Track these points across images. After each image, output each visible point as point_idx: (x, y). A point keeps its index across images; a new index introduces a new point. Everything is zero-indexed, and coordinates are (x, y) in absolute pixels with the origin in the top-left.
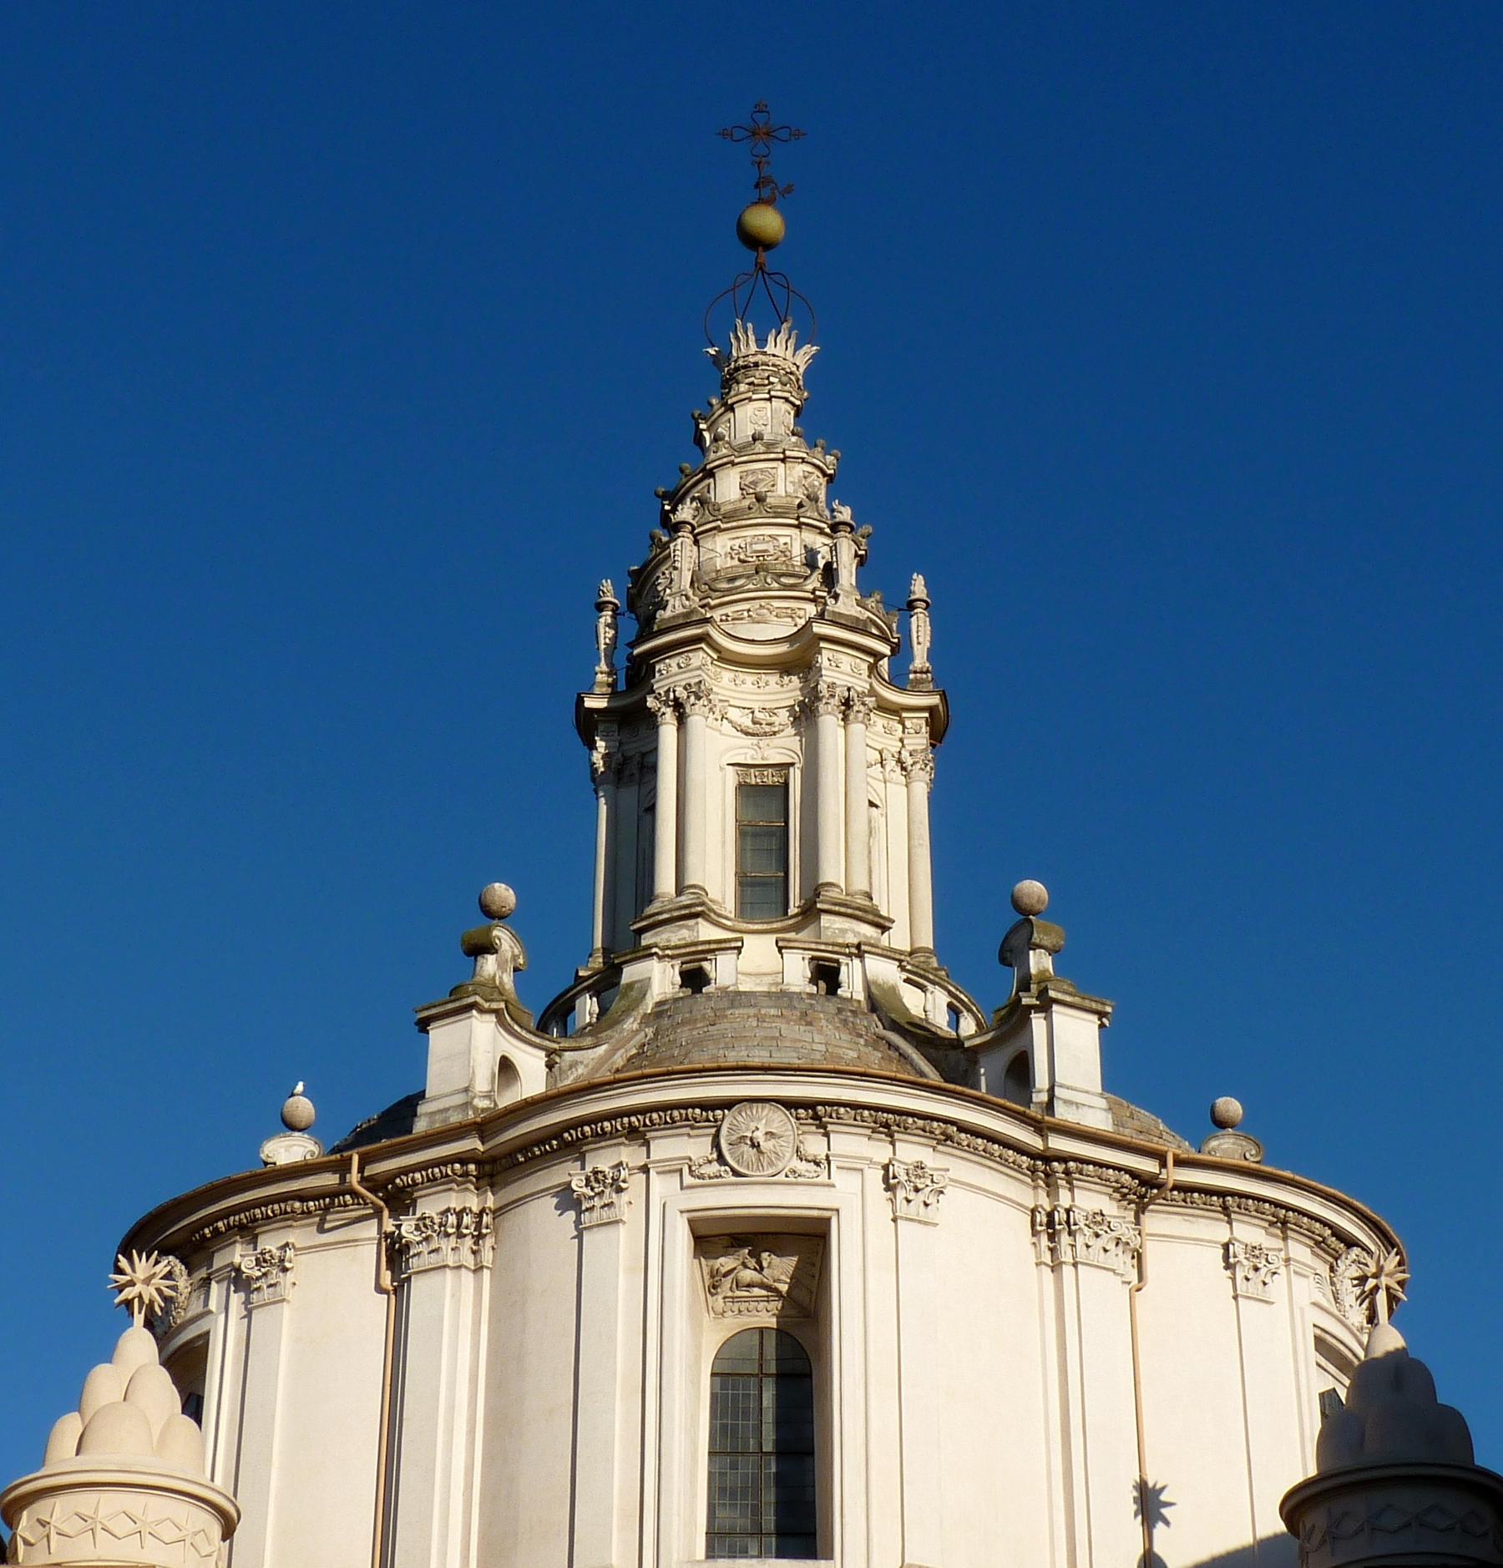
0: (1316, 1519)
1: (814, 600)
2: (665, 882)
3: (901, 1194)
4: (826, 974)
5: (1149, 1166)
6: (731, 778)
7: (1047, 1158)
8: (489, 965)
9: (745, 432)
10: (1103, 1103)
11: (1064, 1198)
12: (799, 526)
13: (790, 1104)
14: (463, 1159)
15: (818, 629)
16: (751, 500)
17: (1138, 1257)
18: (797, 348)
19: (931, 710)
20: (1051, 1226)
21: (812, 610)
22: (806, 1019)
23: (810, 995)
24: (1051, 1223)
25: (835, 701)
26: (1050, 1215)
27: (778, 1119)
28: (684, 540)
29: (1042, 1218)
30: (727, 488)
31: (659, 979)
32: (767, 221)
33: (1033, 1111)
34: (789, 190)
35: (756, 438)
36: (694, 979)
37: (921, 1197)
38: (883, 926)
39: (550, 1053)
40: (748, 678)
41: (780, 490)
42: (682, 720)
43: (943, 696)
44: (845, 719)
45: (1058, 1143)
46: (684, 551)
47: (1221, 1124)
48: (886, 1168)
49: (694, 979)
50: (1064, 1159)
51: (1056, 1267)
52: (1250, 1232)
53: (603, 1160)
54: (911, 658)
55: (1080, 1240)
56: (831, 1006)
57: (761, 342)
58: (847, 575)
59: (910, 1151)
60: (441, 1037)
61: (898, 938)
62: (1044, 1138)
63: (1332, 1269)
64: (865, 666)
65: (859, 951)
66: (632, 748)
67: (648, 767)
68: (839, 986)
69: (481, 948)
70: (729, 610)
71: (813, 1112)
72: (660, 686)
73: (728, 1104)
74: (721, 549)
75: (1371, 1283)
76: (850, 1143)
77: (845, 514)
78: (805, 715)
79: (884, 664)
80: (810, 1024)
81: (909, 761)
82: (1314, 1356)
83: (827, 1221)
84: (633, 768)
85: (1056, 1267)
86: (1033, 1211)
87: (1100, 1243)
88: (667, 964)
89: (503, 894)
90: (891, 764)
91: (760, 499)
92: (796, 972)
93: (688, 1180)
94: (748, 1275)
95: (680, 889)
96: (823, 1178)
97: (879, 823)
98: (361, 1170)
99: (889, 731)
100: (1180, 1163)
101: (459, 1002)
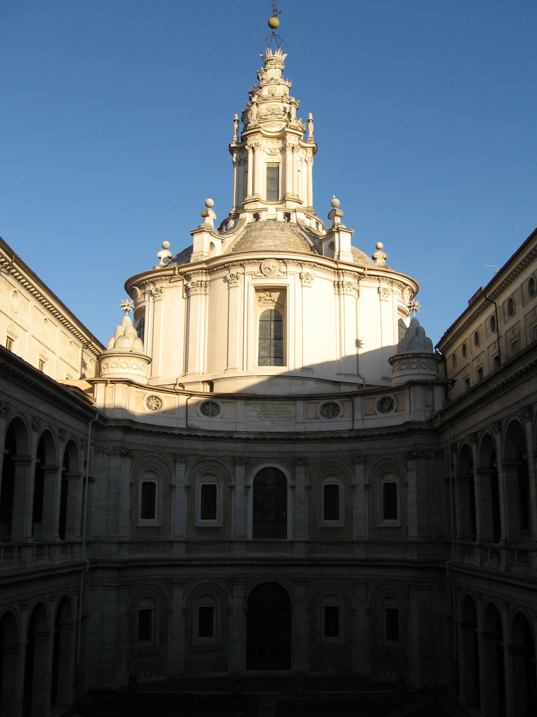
1: (286, 121)
2: (250, 192)
3: (303, 280)
4: (287, 216)
5: (361, 271)
6: (265, 166)
7: (338, 269)
8: (207, 219)
9: (269, 78)
10: (351, 255)
11: (342, 279)
12: (282, 102)
13: (277, 259)
14: (201, 269)
15: (286, 130)
16: (270, 95)
18: (282, 55)
19: (313, 148)
20: (338, 285)
21: (285, 124)
22: (282, 230)
23: (284, 222)
24: (338, 285)
25: (290, 148)
26: (338, 282)
27: (274, 263)
28: (255, 106)
29: (336, 283)
30: (265, 92)
31: (248, 217)
32: (275, 21)
33: (335, 259)
34: (280, 12)
35: (272, 79)
37: (308, 281)
38: (301, 204)
39: (222, 240)
40: (270, 140)
41: (278, 92)
42: (254, 152)
43: (316, 144)
44: (293, 151)
45: (341, 266)
46: (254, 108)
47: (378, 249)
48: (300, 274)
49: (257, 216)
50: (342, 270)
51: (339, 294)
52: (384, 285)
53: (234, 271)
54: (309, 134)
55: (345, 289)
56: (288, 225)
57: (274, 53)
58: (293, 115)
59: (306, 270)
60: (196, 238)
62: (337, 265)
63: (402, 291)
64: (297, 138)
66: (243, 157)
67: (246, 161)
68: (290, 219)
69: (206, 216)
70: (265, 124)
71: (283, 261)
72: (249, 143)
73: (264, 259)
74: (264, 108)
75: (412, 308)
77: (293, 100)
78: (283, 150)
79: (302, 138)
80: (283, 231)
81: (307, 160)
82: (397, 311)
83: (286, 287)
84: (242, 162)
85: (339, 294)
86: (334, 281)
87: (350, 289)
88: (250, 214)
89: (210, 202)
90: (303, 161)
91: (273, 95)
92: (280, 216)
93: (254, 277)
94: (268, 298)
95: (253, 195)
96: (285, 277)
97: (300, 179)
98: (178, 270)
99: (303, 153)
100: (368, 269)
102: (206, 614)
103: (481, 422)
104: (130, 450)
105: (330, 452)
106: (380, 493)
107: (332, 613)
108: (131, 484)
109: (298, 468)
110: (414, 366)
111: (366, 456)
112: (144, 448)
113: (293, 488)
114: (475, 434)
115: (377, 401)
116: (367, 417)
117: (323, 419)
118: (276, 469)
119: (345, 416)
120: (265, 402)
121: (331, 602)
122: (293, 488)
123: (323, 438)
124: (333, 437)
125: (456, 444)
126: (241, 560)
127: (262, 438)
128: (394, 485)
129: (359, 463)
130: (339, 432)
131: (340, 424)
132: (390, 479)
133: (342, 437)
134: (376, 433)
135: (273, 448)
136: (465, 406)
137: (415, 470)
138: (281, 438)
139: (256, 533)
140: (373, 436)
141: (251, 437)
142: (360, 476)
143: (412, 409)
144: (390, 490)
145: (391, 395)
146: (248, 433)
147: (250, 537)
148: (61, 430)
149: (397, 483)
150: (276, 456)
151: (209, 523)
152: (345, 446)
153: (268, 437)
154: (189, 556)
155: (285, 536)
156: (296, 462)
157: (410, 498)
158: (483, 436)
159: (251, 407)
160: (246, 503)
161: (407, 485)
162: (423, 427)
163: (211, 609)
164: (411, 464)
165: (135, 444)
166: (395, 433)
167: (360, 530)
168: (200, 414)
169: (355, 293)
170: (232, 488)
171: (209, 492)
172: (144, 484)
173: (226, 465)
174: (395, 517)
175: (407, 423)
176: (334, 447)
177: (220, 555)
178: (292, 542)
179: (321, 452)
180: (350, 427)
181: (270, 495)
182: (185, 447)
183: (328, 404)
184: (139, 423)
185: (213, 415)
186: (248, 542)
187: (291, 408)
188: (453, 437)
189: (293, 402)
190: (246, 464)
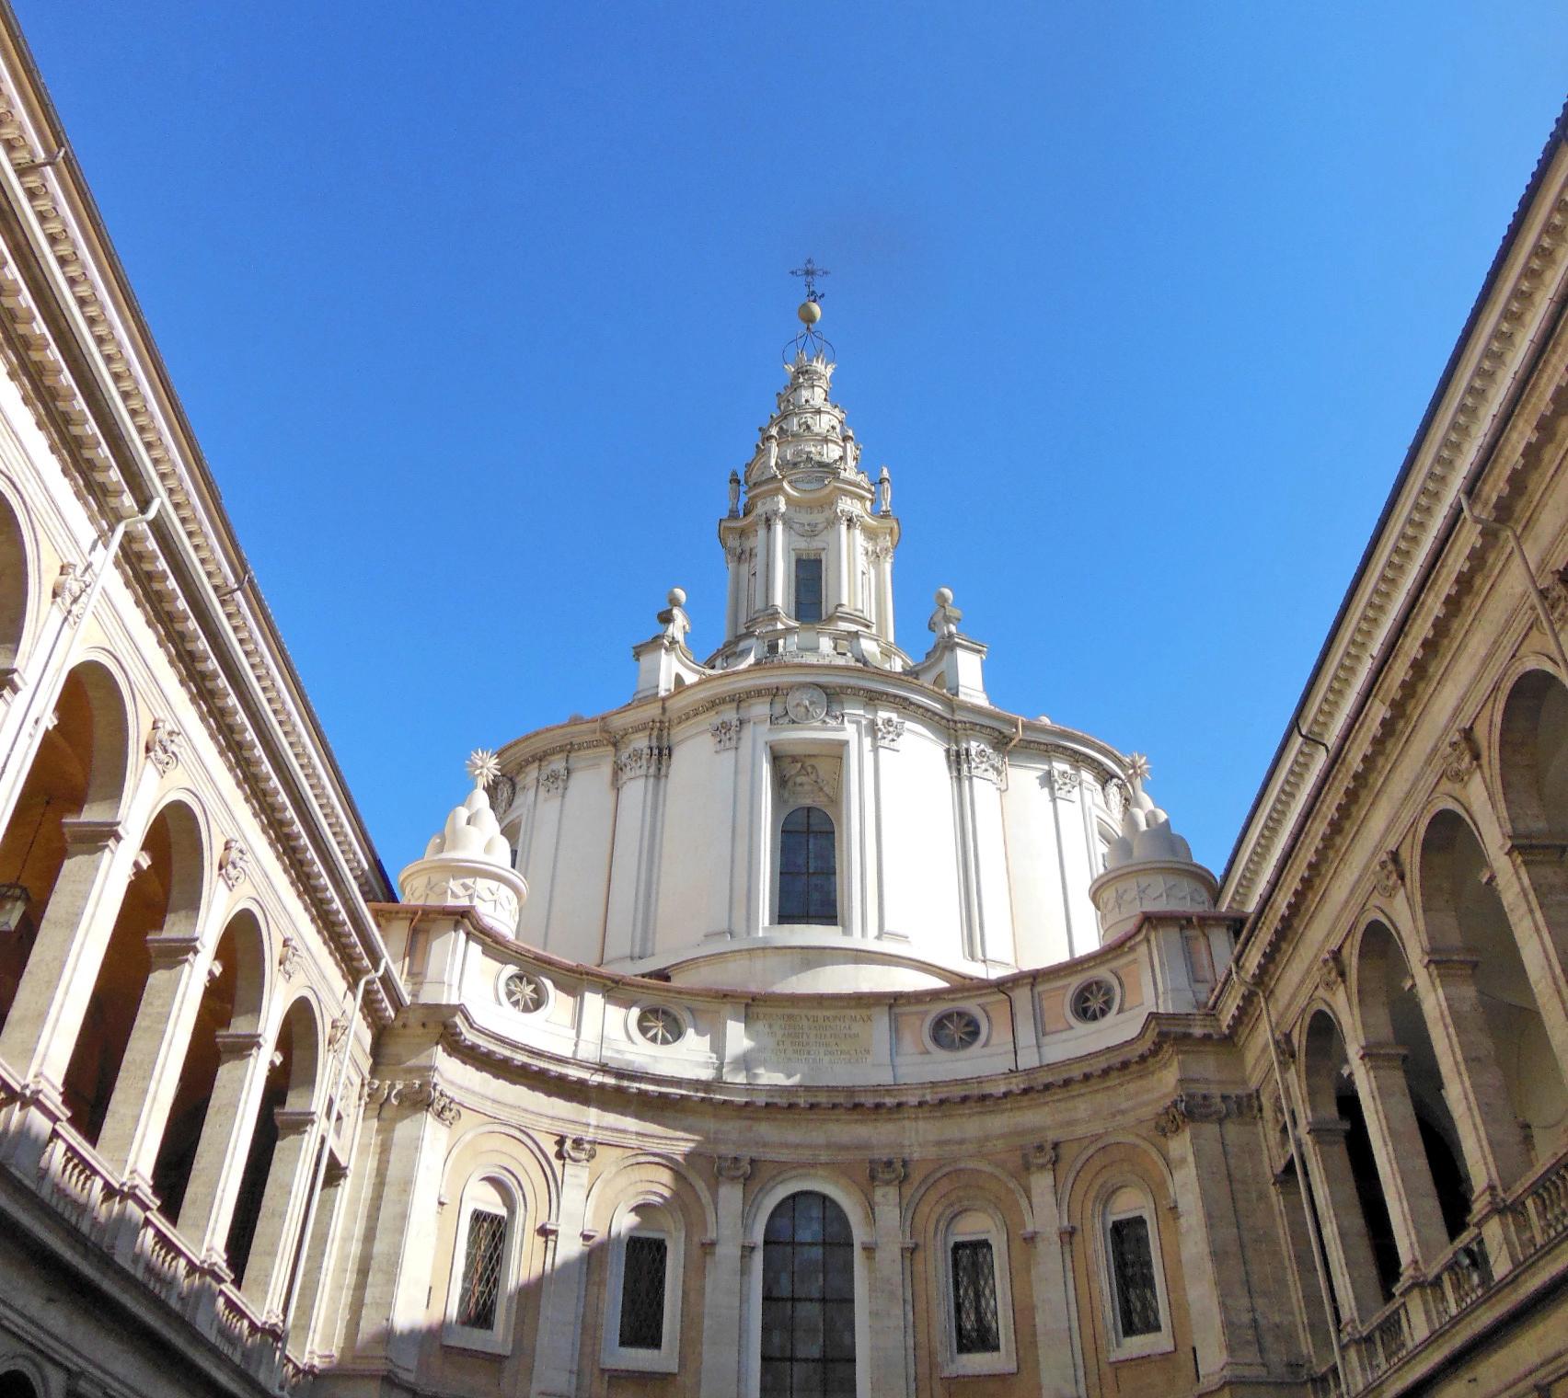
0: (1110, 894)
103: (1347, 902)
104: (452, 1101)
105: (962, 1142)
106: (1099, 1250)
108: (441, 1204)
111: (1056, 1146)
112: (489, 1108)
114: (1336, 955)
116: (1047, 1039)
117: (940, 1054)
119: (994, 1040)
120: (795, 1012)
123: (942, 1102)
124: (965, 1099)
125: (1288, 1037)
128: (1140, 1222)
129: (1042, 1167)
130: (980, 1080)
131: (983, 1062)
133: (991, 1095)
134: (1077, 1073)
136: (1296, 884)
137: (1191, 1158)
138: (835, 1106)
140: (1067, 1083)
141: (761, 1100)
143: (1161, 989)
148: (285, 943)
149: (1146, 1216)
151: (640, 1358)
152: (998, 1123)
153: (801, 1101)
158: (1357, 945)
161: (1174, 1209)
162: (1198, 1031)
164: (1181, 1145)
165: (467, 1090)
166: (1125, 1065)
172: (478, 1217)
175: (1153, 1016)
176: (970, 1126)
180: (1005, 1064)
182: (593, 1122)
183: (948, 1016)
184: (481, 1031)
185: (665, 1042)
187: (856, 1028)
188: (1278, 1024)
189: (864, 1012)
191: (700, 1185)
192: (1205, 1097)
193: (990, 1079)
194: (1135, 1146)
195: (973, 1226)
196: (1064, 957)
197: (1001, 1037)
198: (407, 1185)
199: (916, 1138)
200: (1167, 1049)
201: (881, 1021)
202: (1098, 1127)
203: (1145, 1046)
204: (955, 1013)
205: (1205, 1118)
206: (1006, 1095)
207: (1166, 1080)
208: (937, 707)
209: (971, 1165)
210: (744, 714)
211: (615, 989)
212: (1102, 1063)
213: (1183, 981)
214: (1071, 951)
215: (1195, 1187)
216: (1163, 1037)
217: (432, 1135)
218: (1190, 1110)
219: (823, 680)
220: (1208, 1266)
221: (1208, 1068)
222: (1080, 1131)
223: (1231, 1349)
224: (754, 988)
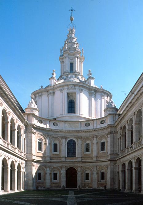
11: (91, 91)
17: (95, 95)
36: (67, 77)
42: (66, 58)
45: (91, 88)
51: (90, 96)
59: (81, 88)
61: (80, 74)
62: (90, 87)
65: (78, 75)
66: (63, 61)
69: (53, 74)
76: (77, 87)
101: (52, 78)
102: (55, 175)
107: (87, 175)
109: (79, 139)
110: (111, 111)
113: (78, 144)
115: (100, 121)
117: (86, 127)
118: (73, 140)
121: (87, 172)
122: (78, 144)
124: (88, 131)
126: (64, 162)
127: (69, 132)
128: (104, 142)
130: (90, 130)
132: (103, 141)
135: (72, 134)
139: (67, 156)
142: (95, 141)
144: (103, 144)
145: (104, 119)
146: (66, 130)
147: (66, 156)
150: (73, 136)
152: (92, 133)
154: (51, 160)
155: (75, 157)
156: (78, 138)
157: (108, 147)
159: (66, 124)
160: (65, 148)
161: (108, 141)
162: (113, 126)
163: (56, 174)
166: (105, 128)
167: (95, 154)
168: (53, 125)
169: (94, 95)
170: (61, 144)
171: (55, 145)
172: (39, 142)
173: (60, 138)
174: (104, 150)
177: (59, 161)
178: (77, 158)
179: (85, 135)
180: (93, 128)
181: (71, 146)
183: (87, 123)
185: (56, 126)
186: (66, 158)
187: (77, 124)
190: (65, 138)
191: (61, 139)
192: (112, 132)
193: (91, 129)
194: (105, 136)
195: (88, 142)
196: (100, 117)
197: (92, 125)
198: (31, 140)
199: (83, 135)
200: (109, 127)
201: (79, 123)
202: (101, 134)
203: (107, 127)
204: (88, 123)
205: (112, 133)
206: (92, 131)
207: (109, 130)
208: (88, 87)
209: (88, 137)
210: (64, 88)
211: (50, 120)
212: (103, 128)
213: (112, 120)
214: (101, 116)
215: (110, 139)
216: (109, 126)
217: (33, 135)
218: (111, 133)
219: (74, 84)
220: (110, 146)
221: (113, 129)
222: (99, 134)
223: (111, 152)
224: (66, 120)
